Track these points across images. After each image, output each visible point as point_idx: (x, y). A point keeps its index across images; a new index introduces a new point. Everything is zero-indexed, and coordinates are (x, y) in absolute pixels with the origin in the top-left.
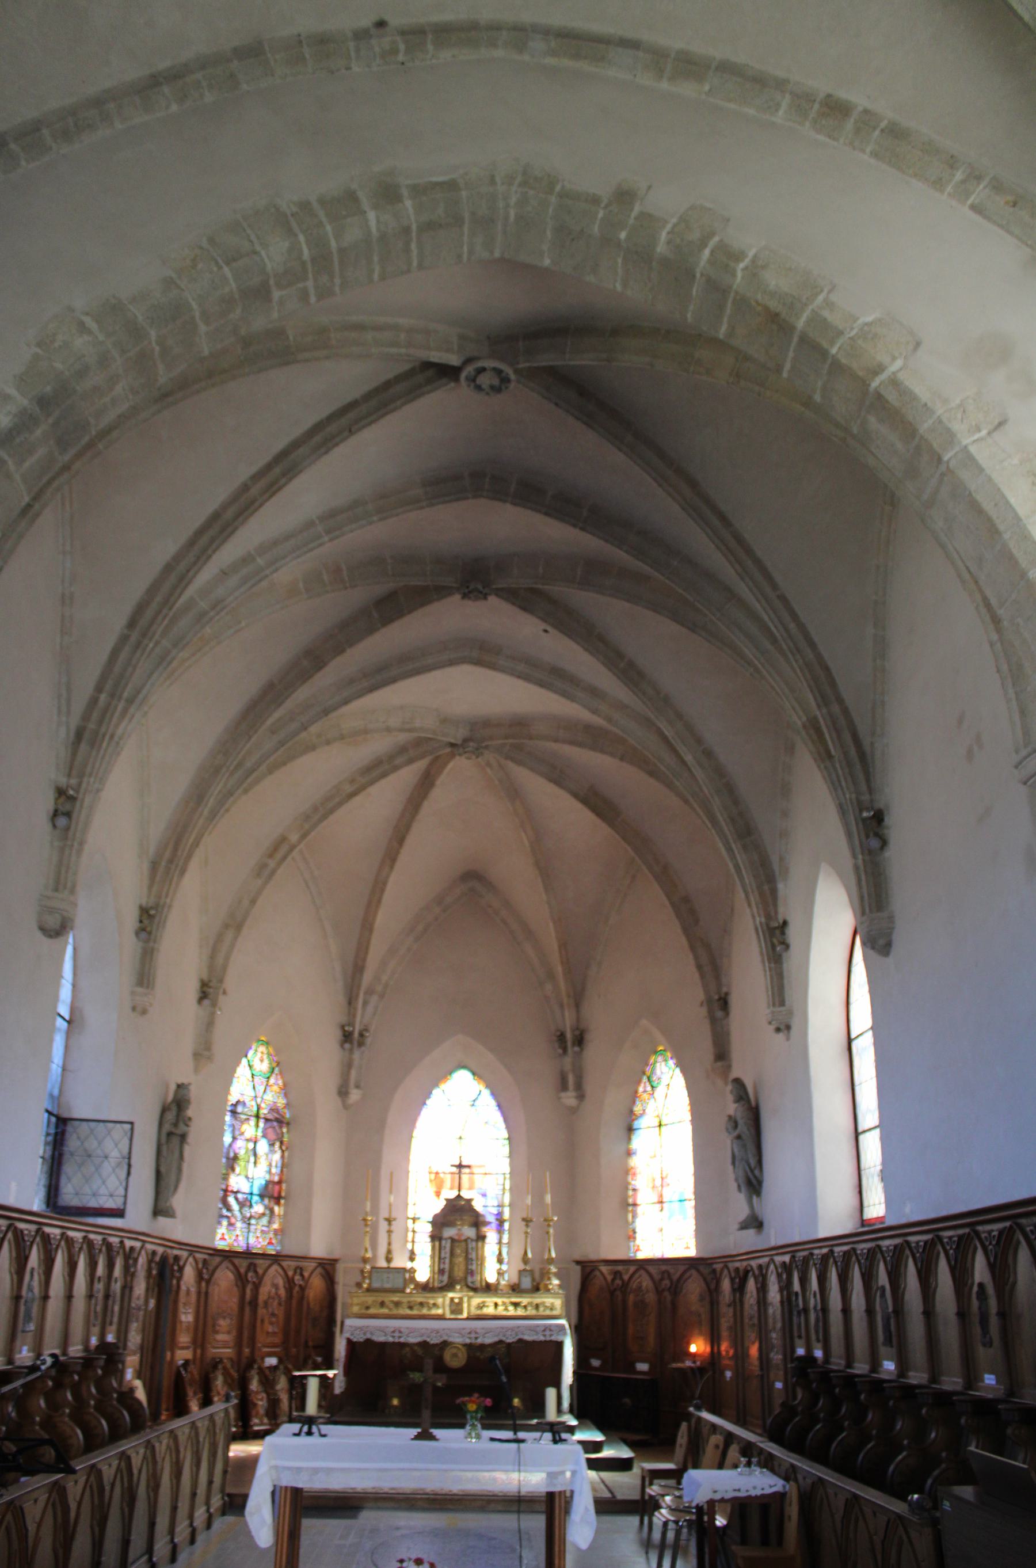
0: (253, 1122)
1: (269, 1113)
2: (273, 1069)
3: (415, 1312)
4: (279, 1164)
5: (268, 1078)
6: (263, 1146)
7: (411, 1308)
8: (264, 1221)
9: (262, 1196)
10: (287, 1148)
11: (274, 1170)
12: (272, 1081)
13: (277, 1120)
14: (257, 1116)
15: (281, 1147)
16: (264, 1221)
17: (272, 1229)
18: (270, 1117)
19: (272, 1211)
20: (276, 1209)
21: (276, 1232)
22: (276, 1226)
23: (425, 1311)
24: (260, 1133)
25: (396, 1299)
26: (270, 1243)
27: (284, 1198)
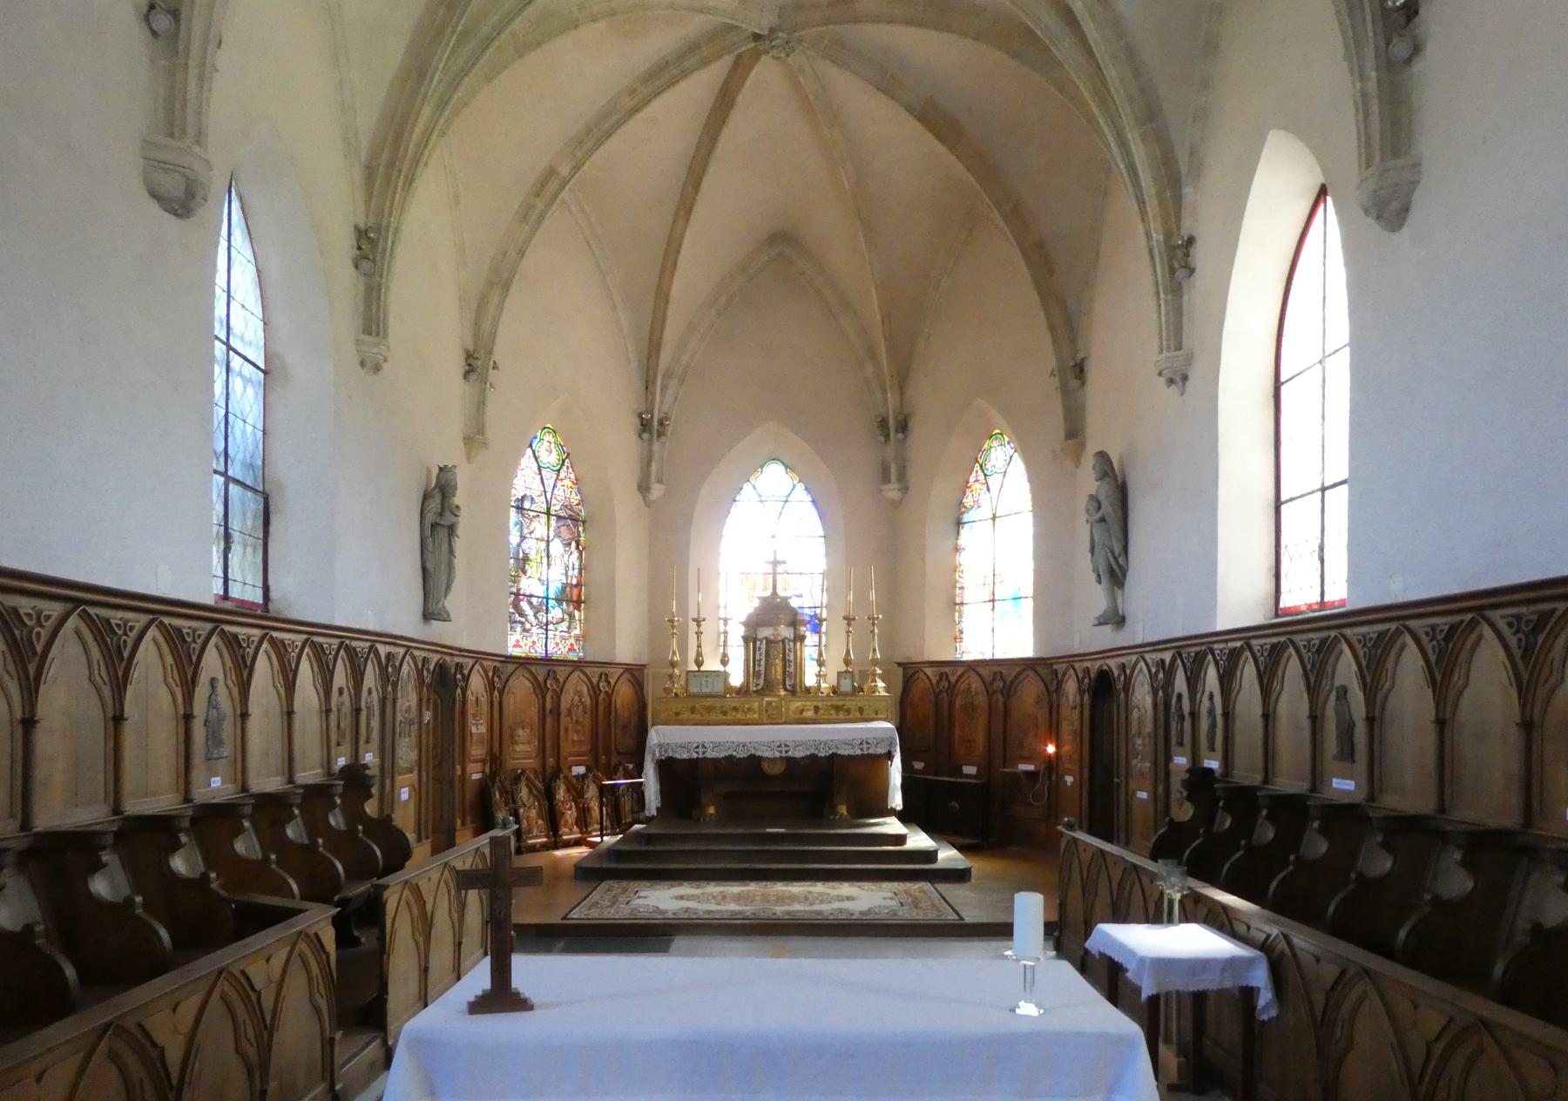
0: (544, 518)
1: (561, 509)
2: (564, 461)
3: (729, 717)
4: (577, 566)
5: (559, 471)
6: (557, 547)
7: (725, 713)
8: (564, 626)
9: (559, 601)
10: (583, 549)
11: (570, 573)
12: (562, 475)
13: (570, 518)
14: (548, 513)
15: (577, 548)
16: (564, 626)
17: (572, 634)
18: (562, 514)
19: (571, 616)
20: (576, 612)
21: (577, 638)
22: (577, 632)
23: (739, 716)
24: (552, 534)
25: (707, 704)
26: (571, 649)
27: (584, 602)
